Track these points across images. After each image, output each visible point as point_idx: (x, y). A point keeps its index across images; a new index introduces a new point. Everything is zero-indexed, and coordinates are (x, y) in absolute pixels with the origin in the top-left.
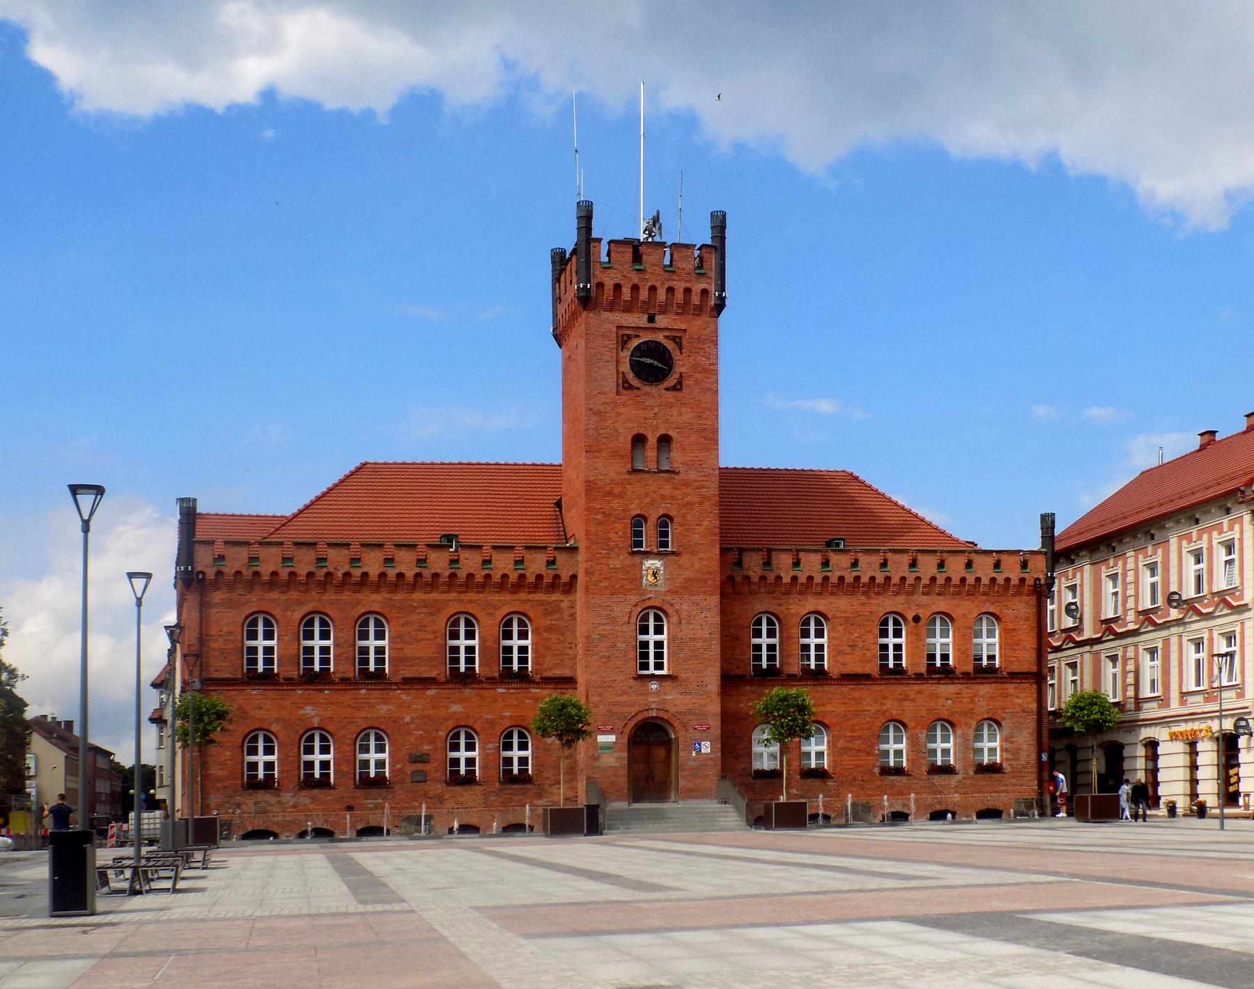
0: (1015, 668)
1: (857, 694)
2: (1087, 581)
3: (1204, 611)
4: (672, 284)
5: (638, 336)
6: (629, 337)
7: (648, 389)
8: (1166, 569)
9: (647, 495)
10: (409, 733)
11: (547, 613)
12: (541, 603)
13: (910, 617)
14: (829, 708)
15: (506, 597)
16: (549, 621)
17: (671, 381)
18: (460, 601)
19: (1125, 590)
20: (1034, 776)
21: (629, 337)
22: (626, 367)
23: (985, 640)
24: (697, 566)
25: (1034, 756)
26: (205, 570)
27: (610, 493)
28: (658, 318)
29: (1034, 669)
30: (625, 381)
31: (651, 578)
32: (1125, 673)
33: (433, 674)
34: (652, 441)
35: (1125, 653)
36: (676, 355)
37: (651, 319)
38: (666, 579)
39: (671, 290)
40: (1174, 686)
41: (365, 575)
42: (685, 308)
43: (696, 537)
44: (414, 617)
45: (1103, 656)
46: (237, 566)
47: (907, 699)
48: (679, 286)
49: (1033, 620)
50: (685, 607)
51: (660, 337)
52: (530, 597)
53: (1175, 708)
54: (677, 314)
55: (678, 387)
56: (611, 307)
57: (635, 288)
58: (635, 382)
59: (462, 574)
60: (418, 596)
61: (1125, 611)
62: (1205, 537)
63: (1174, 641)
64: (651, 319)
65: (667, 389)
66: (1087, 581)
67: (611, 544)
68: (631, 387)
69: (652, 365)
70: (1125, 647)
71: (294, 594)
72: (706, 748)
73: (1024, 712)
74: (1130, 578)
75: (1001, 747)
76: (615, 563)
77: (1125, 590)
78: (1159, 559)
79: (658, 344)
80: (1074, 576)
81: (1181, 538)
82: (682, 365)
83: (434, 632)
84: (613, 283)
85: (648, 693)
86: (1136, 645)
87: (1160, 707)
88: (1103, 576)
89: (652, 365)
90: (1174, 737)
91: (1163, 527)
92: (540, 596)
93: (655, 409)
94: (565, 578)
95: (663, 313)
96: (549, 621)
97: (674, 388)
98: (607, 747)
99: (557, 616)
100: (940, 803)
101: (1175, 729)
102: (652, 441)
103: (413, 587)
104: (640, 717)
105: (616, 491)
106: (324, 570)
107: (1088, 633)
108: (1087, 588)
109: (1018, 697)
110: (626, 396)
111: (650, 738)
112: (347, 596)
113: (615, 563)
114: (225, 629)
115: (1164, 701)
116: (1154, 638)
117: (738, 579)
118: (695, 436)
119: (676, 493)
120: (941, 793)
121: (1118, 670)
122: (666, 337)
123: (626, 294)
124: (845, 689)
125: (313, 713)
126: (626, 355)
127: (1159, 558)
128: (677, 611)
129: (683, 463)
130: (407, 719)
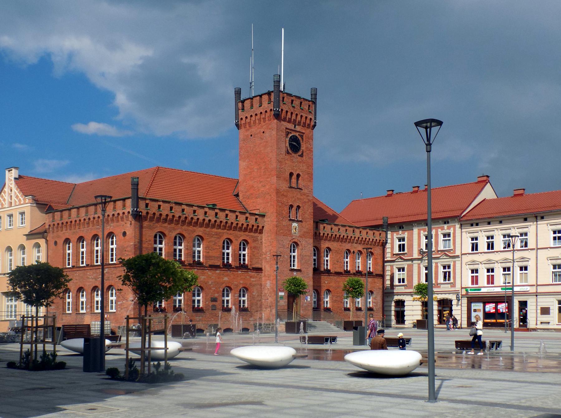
1: (338, 280)
4: (303, 114)
7: (293, 154)
10: (210, 289)
11: (255, 241)
12: (252, 237)
13: (352, 251)
15: (242, 233)
16: (253, 245)
17: (300, 153)
18: (228, 233)
22: (288, 145)
26: (142, 211)
29: (382, 273)
37: (295, 127)
39: (302, 116)
42: (304, 126)
44: (213, 239)
51: (297, 134)
57: (292, 113)
58: (290, 151)
60: (215, 230)
64: (295, 127)
69: (295, 145)
79: (297, 137)
82: (303, 147)
83: (219, 246)
89: (295, 145)
92: (252, 234)
94: (260, 228)
95: (298, 125)
96: (253, 245)
98: (282, 297)
99: (257, 242)
103: (213, 226)
106: (185, 216)
110: (287, 157)
112: (191, 228)
114: (148, 239)
118: (306, 176)
119: (301, 197)
124: (335, 277)
130: (210, 283)
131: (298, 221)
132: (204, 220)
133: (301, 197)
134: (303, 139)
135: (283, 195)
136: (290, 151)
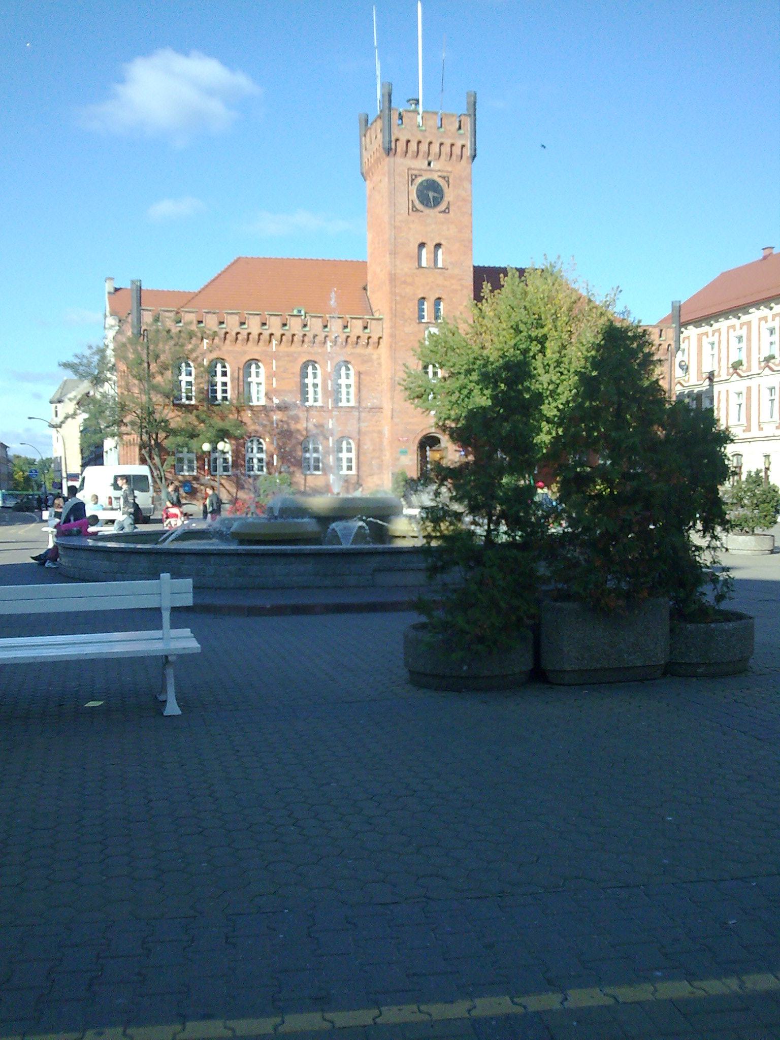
5: (420, 175)
8: (749, 340)
9: (428, 284)
11: (364, 362)
12: (360, 355)
17: (442, 206)
22: (414, 196)
30: (414, 206)
51: (435, 177)
52: (353, 351)
55: (446, 211)
59: (310, 335)
65: (440, 212)
68: (417, 210)
79: (434, 182)
82: (449, 195)
83: (293, 373)
93: (431, 224)
97: (444, 212)
122: (440, 177)
126: (414, 189)
134: (448, 182)
135: (405, 282)
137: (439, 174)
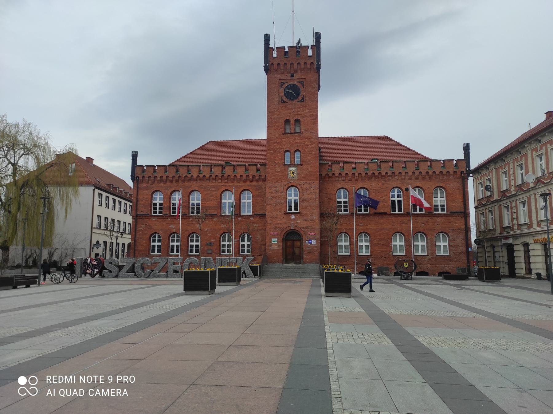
0: (454, 210)
1: (382, 221)
2: (494, 176)
3: (545, 182)
4: (299, 61)
6: (284, 83)
8: (527, 166)
13: (404, 189)
14: (369, 227)
15: (241, 183)
17: (300, 98)
18: (226, 186)
19: (509, 177)
20: (465, 258)
21: (284, 83)
22: (282, 95)
23: (439, 199)
24: (310, 169)
25: (465, 249)
27: (276, 142)
28: (295, 75)
29: (463, 210)
30: (282, 100)
31: (292, 175)
32: (512, 213)
33: (216, 213)
34: (292, 122)
35: (511, 205)
36: (301, 89)
38: (297, 175)
40: (534, 218)
41: (192, 176)
43: (309, 158)
44: (209, 192)
45: (502, 207)
46: (149, 174)
47: (404, 223)
48: (302, 62)
49: (461, 188)
50: (305, 185)
51: (295, 82)
53: (535, 228)
54: (301, 73)
56: (276, 72)
58: (286, 100)
59: (226, 176)
60: (211, 184)
61: (510, 187)
62: (544, 148)
63: (532, 197)
64: (292, 76)
66: (494, 176)
67: (277, 162)
68: (284, 102)
70: (511, 202)
71: (168, 184)
72: (314, 242)
73: (459, 229)
74: (512, 172)
75: (449, 244)
76: (278, 169)
77: (509, 177)
78: (523, 162)
80: (489, 174)
81: (532, 151)
83: (216, 197)
84: (277, 63)
85: (291, 220)
86: (516, 201)
87: (529, 228)
88: (501, 173)
90: (536, 242)
91: (524, 147)
92: (254, 183)
95: (296, 73)
97: (300, 101)
100: (421, 268)
101: (536, 238)
102: (292, 122)
104: (287, 229)
105: (278, 142)
106: (178, 175)
107: (496, 197)
108: (494, 179)
109: (455, 223)
111: (292, 237)
113: (278, 169)
114: (145, 197)
115: (530, 226)
116: (524, 197)
117: (330, 175)
119: (301, 141)
120: (421, 264)
121: (509, 212)
123: (282, 66)
124: (376, 219)
125: (174, 227)
126: (282, 89)
127: (523, 161)
128: (302, 187)
129: (304, 130)
130: (206, 230)
131: (295, 165)
132: (198, 176)
133: (301, 141)
135: (276, 142)
136: (286, 100)
137: (298, 80)
